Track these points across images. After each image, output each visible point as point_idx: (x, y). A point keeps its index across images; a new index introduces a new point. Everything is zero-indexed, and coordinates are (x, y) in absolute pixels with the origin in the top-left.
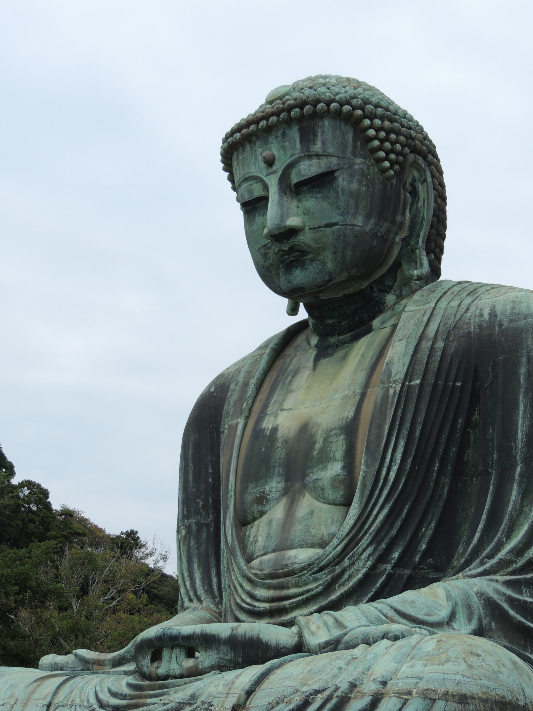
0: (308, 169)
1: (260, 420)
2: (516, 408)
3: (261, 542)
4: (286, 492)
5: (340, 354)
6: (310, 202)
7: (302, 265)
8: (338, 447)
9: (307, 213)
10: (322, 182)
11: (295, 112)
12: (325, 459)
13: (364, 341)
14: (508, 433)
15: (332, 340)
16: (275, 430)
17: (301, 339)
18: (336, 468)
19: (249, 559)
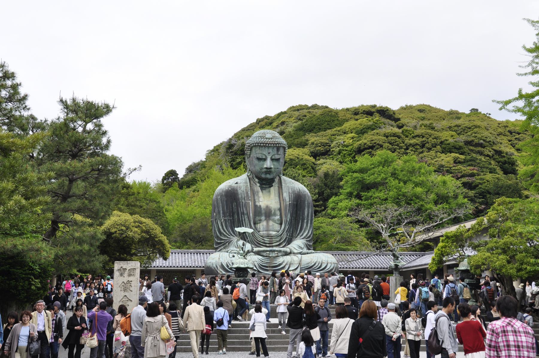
0: (277, 157)
1: (255, 202)
2: (305, 209)
3: (261, 229)
4: (265, 219)
5: (267, 190)
6: (275, 163)
7: (270, 174)
8: (278, 213)
9: (274, 165)
10: (278, 160)
11: (277, 145)
12: (275, 215)
13: (272, 188)
14: (304, 213)
15: (264, 186)
16: (260, 206)
17: (252, 182)
18: (278, 217)
19: (259, 232)
